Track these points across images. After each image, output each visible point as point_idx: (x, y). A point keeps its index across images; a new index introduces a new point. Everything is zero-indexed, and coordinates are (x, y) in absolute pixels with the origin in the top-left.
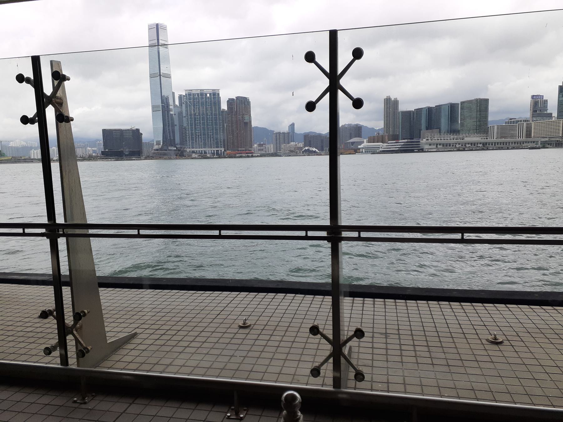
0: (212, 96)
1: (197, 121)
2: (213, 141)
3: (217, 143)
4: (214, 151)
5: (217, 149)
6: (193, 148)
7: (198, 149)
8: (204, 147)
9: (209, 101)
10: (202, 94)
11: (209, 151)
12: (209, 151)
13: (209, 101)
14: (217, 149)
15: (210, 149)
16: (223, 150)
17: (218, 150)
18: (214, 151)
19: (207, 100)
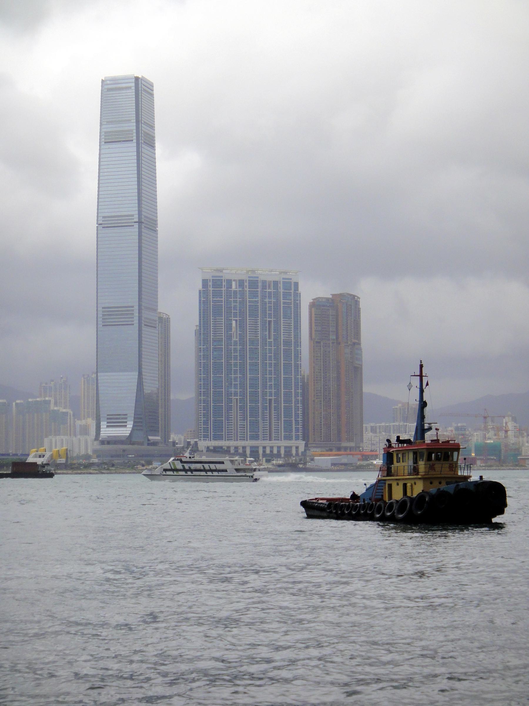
0: (282, 290)
1: (236, 358)
2: (278, 418)
3: (288, 424)
4: (279, 447)
5: (288, 443)
6: (217, 437)
7: (232, 443)
8: (253, 438)
9: (270, 303)
10: (253, 283)
11: (264, 448)
12: (264, 448)
13: (270, 303)
14: (288, 443)
15: (267, 443)
16: (301, 444)
17: (291, 447)
18: (279, 447)
19: (267, 300)
